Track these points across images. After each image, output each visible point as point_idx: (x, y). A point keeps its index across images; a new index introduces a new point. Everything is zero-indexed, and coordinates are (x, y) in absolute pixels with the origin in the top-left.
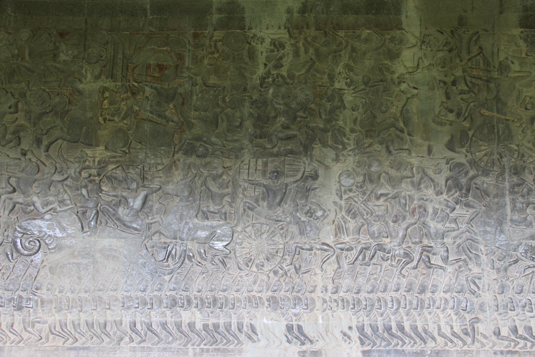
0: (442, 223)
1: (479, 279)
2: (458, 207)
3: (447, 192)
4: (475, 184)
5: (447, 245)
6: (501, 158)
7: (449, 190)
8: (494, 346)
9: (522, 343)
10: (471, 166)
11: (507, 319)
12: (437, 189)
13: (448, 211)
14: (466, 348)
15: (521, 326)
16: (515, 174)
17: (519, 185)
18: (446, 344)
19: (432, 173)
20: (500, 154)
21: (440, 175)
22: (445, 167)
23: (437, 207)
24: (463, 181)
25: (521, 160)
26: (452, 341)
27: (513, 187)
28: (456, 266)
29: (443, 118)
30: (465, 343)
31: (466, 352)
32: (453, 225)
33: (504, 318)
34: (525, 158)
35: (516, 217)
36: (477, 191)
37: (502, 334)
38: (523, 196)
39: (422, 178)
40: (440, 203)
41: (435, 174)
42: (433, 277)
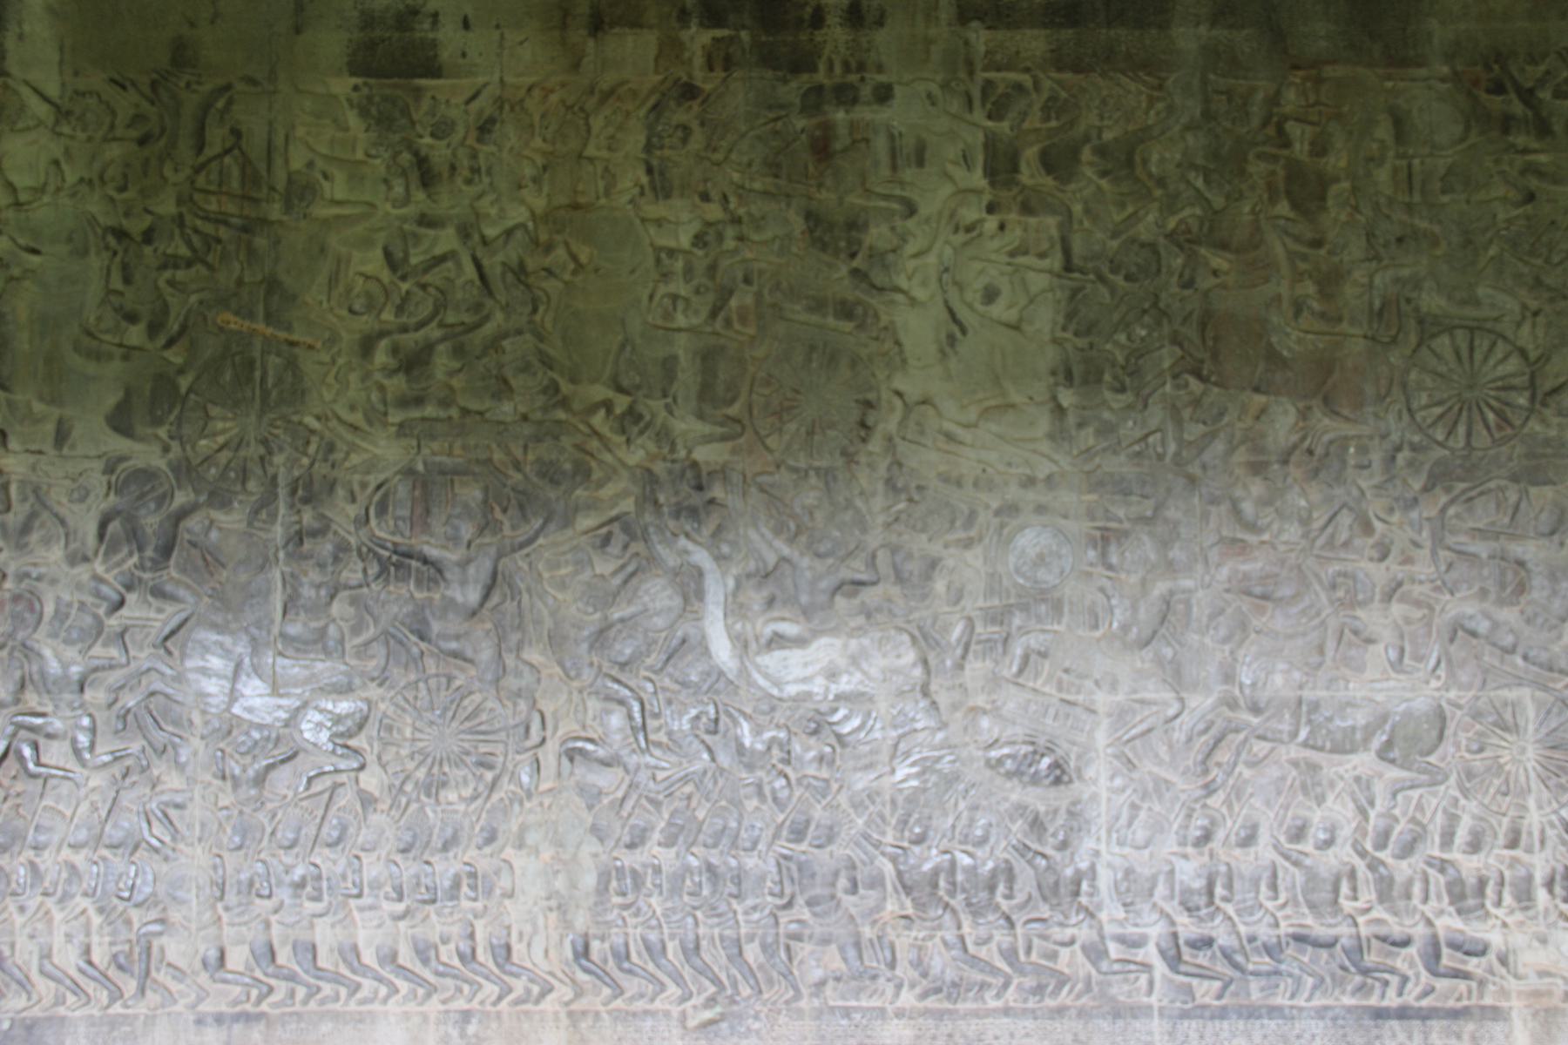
0: (79, 646)
1: (178, 806)
2: (132, 598)
3: (106, 554)
4: (188, 531)
5: (91, 710)
6: (270, 453)
7: (112, 549)
8: (200, 1000)
9: (282, 988)
10: (178, 479)
11: (245, 923)
12: (73, 546)
13: (101, 612)
14: (117, 1008)
15: (283, 943)
16: (306, 501)
17: (314, 534)
18: (60, 1001)
19: (64, 500)
20: (264, 442)
21: (84, 506)
22: (97, 481)
23: (67, 597)
24: (151, 521)
25: (326, 460)
26: (77, 989)
27: (299, 537)
28: (117, 770)
29: (107, 337)
30: (117, 994)
31: (114, 1023)
32: (114, 652)
33: (237, 920)
34: (338, 456)
35: (294, 629)
36: (194, 552)
37: (230, 965)
38: (321, 566)
39: (33, 516)
40: (79, 587)
41: (71, 501)
42: (44, 803)
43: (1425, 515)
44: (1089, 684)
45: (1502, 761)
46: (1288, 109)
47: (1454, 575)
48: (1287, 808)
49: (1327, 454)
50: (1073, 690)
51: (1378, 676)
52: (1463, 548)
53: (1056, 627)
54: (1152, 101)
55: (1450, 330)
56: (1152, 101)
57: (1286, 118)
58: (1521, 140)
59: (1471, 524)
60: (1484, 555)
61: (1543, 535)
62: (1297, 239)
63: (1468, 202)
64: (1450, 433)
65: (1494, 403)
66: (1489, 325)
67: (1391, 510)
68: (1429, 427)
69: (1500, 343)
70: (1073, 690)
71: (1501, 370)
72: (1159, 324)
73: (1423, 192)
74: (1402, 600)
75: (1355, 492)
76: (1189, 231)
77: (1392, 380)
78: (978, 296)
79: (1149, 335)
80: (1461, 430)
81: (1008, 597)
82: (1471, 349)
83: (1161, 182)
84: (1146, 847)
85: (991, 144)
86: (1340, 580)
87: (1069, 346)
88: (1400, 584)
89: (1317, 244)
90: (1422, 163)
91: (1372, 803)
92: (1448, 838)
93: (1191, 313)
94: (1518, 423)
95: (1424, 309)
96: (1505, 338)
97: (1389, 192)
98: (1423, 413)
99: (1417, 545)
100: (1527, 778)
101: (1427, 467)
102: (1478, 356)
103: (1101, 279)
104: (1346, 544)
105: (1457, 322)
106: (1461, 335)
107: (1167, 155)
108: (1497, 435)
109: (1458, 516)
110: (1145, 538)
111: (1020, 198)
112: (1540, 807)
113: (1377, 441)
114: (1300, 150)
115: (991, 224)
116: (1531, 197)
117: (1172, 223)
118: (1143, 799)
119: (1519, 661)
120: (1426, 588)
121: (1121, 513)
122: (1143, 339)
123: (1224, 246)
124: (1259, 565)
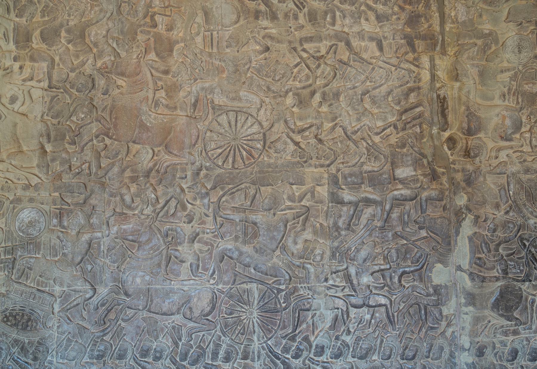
43: (211, 201)
44: (52, 282)
45: (242, 318)
46: (156, 10)
47: (223, 230)
48: (141, 341)
49: (166, 172)
50: (44, 285)
51: (186, 278)
52: (228, 216)
53: (37, 256)
54: (92, 6)
55: (227, 112)
56: (92, 6)
57: (155, 14)
58: (265, 23)
59: (233, 205)
60: (238, 220)
61: (266, 210)
62: (157, 70)
63: (238, 51)
64: (224, 162)
65: (245, 147)
66: (244, 110)
67: (195, 199)
68: (215, 159)
69: (249, 118)
70: (44, 285)
71: (250, 131)
72: (91, 112)
73: (218, 48)
74: (199, 242)
75: (178, 190)
76: (107, 68)
77: (198, 136)
78: (8, 100)
79: (86, 117)
80: (230, 160)
81: (16, 242)
82: (236, 121)
83: (96, 45)
84: (73, 360)
85: (16, 29)
86: (170, 232)
87: (49, 123)
88: (198, 234)
89: (166, 72)
90: (218, 33)
91: (180, 340)
92: (215, 355)
93: (106, 107)
94: (257, 156)
95: (217, 103)
96: (252, 116)
97: (202, 47)
98: (212, 152)
99: (207, 216)
100: (254, 326)
101: (213, 178)
102: (239, 125)
103: (66, 91)
104: (173, 215)
105: (229, 108)
106: (232, 115)
107: (99, 32)
108: (247, 163)
109: (226, 201)
110: (79, 213)
111: (29, 54)
112: (259, 340)
113: (190, 166)
114: (161, 29)
115: (17, 65)
116: (267, 49)
117: (99, 64)
118: (73, 337)
119: (253, 271)
120: (210, 235)
121: (69, 201)
122: (82, 119)
123: (122, 74)
124: (131, 226)
